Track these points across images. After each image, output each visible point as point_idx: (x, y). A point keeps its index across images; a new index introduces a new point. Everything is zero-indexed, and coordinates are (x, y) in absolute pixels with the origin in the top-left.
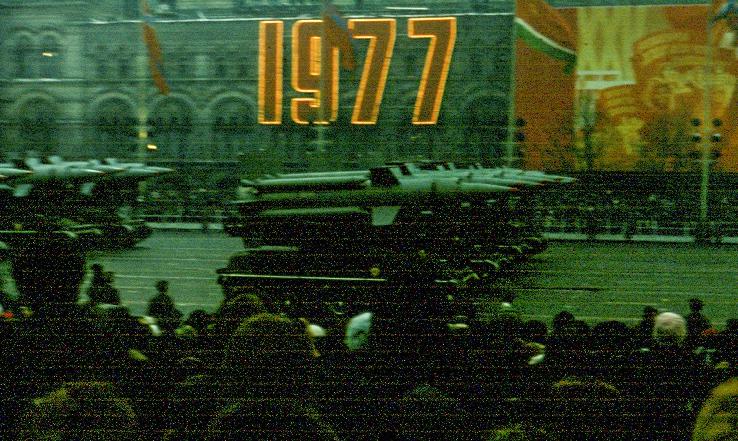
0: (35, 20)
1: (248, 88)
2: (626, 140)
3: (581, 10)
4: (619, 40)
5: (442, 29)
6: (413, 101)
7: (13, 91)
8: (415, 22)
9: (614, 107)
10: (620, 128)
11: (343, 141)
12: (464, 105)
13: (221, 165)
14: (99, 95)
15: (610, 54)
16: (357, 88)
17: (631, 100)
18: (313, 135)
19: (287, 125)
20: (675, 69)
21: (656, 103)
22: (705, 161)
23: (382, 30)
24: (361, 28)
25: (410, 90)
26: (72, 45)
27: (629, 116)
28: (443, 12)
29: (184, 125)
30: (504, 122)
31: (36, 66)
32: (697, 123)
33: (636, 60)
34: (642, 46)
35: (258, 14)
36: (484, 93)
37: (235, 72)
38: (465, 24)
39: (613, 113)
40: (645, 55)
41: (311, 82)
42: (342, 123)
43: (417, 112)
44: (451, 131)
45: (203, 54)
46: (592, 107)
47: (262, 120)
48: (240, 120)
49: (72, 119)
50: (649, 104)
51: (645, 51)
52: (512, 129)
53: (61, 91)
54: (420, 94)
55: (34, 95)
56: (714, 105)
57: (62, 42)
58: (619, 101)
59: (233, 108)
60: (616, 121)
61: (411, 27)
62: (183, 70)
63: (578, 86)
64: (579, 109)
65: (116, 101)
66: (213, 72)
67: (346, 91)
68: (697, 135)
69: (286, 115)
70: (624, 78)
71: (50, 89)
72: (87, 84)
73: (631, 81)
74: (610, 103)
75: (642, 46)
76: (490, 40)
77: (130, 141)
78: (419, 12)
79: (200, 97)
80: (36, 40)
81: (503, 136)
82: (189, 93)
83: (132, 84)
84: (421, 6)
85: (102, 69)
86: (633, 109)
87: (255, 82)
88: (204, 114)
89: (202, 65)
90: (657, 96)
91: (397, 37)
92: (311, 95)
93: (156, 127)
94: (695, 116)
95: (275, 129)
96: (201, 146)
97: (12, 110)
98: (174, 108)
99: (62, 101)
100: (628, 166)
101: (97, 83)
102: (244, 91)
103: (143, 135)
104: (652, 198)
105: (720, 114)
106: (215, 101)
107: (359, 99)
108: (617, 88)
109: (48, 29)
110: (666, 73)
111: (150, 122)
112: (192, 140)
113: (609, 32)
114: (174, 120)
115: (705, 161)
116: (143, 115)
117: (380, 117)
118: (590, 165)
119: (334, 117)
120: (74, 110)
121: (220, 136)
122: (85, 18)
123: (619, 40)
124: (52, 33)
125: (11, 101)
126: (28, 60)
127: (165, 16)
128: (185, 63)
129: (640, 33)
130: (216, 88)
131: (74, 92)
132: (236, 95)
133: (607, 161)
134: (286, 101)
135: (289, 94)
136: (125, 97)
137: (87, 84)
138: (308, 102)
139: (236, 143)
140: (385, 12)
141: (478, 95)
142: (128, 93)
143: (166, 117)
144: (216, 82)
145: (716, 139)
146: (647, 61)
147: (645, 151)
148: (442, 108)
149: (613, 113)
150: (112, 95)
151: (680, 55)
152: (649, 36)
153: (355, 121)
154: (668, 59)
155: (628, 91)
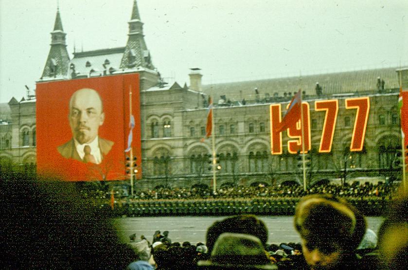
0: (160, 111)
1: (265, 137)
5: (363, 104)
6: (350, 139)
7: (149, 145)
8: (348, 101)
11: (315, 161)
12: (377, 140)
13: (253, 175)
14: (192, 144)
16: (321, 135)
18: (300, 159)
19: (286, 155)
23: (332, 106)
24: (320, 105)
25: (348, 134)
26: (177, 121)
28: (362, 95)
29: (235, 157)
30: (400, 148)
31: (161, 133)
35: (267, 101)
36: (386, 133)
37: (258, 129)
38: (375, 101)
41: (298, 133)
42: (313, 152)
44: (370, 154)
45: (241, 122)
47: (272, 152)
48: (262, 153)
49: (177, 156)
53: (172, 143)
55: (160, 146)
57: (172, 120)
59: (258, 147)
61: (346, 103)
62: (232, 130)
65: (200, 147)
66: (248, 130)
67: (315, 136)
69: (285, 148)
71: (168, 142)
72: (185, 139)
76: (388, 107)
77: (207, 165)
78: (350, 96)
79: (242, 143)
80: (160, 120)
81: (400, 154)
82: (236, 142)
85: (192, 131)
87: (268, 134)
88: (244, 151)
89: (242, 128)
92: (298, 139)
93: (220, 158)
95: (280, 156)
96: (243, 166)
97: (149, 154)
98: (229, 148)
99: (173, 148)
101: (190, 139)
102: (263, 139)
103: (214, 162)
106: (249, 144)
107: (322, 140)
111: (218, 156)
112: (239, 164)
114: (229, 154)
116: (214, 154)
117: (332, 148)
119: (310, 149)
120: (179, 152)
121: (252, 161)
122: (184, 108)
125: (147, 149)
126: (156, 128)
127: (222, 105)
128: (233, 127)
130: (250, 138)
131: (180, 143)
132: (260, 141)
134: (285, 143)
135: (286, 139)
136: (203, 145)
137: (185, 139)
138: (296, 143)
139: (260, 163)
140: (332, 97)
141: (382, 135)
142: (206, 143)
143: (225, 153)
144: (248, 135)
148: (365, 140)
150: (198, 144)
153: (320, 151)
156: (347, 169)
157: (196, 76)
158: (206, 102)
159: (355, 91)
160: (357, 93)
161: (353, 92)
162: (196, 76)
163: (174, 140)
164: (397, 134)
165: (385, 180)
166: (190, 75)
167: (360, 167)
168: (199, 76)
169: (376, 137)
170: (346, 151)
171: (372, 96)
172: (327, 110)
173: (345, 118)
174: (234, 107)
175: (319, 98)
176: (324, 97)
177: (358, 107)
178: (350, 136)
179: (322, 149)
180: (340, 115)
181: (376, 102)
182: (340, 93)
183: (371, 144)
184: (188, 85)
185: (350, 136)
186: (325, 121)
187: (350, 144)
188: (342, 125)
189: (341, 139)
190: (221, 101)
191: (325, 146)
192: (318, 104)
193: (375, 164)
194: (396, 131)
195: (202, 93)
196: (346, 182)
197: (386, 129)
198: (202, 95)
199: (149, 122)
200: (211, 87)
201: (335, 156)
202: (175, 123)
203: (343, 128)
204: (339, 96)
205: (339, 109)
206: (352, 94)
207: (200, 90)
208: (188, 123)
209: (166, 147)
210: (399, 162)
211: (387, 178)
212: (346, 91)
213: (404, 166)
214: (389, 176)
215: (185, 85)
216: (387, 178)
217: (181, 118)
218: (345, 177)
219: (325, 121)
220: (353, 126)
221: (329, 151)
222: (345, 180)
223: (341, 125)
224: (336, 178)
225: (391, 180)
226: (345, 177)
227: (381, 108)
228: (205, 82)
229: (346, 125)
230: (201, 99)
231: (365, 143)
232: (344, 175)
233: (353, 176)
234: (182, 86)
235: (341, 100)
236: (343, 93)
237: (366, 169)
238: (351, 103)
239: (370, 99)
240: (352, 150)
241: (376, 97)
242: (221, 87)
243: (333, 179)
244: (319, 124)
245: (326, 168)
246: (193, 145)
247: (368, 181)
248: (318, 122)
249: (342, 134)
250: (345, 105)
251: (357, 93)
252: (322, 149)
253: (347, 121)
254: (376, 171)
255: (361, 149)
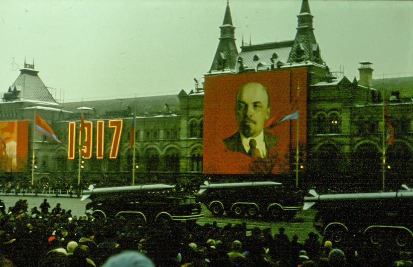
0: (327, 106)
14: (360, 141)
53: (339, 139)
55: (327, 142)
57: (340, 116)
80: (328, 116)
83: (377, 136)
103: (384, 161)
109: (333, 110)
120: (347, 149)
124: (336, 112)
150: (367, 141)
157: (366, 71)
158: (375, 97)
162: (366, 71)
163: (342, 136)
166: (359, 70)
168: (370, 71)
174: (406, 103)
184: (358, 79)
190: (393, 98)
195: (372, 89)
198: (373, 91)
199: (316, 117)
200: (383, 83)
202: (343, 119)
207: (371, 85)
208: (356, 120)
209: (333, 143)
215: (355, 79)
217: (349, 114)
228: (376, 76)
230: (370, 96)
234: (352, 81)
242: (393, 81)
246: (361, 143)
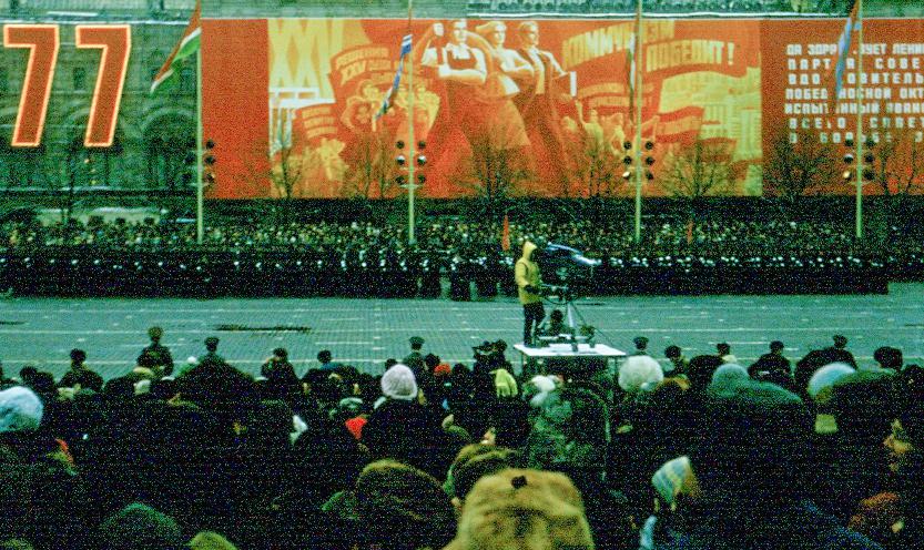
2: (327, 163)
3: (272, 22)
4: (315, 57)
5: (115, 39)
6: (84, 120)
9: (315, 127)
10: (318, 150)
12: (143, 127)
15: (305, 64)
17: (331, 120)
20: (377, 86)
21: (354, 119)
22: (411, 187)
23: (43, 39)
25: (81, 107)
27: (329, 137)
28: (115, 19)
30: (192, 144)
32: (401, 145)
33: (334, 78)
34: (340, 61)
36: (165, 111)
38: (143, 34)
39: (311, 134)
40: (344, 72)
43: (88, 133)
44: (129, 155)
46: (289, 128)
50: (350, 125)
51: (342, 67)
52: (200, 152)
54: (93, 111)
56: (418, 126)
58: (317, 121)
60: (315, 143)
61: (78, 36)
63: (271, 105)
64: (273, 130)
68: (401, 158)
70: (322, 96)
73: (332, 101)
74: (307, 124)
75: (340, 61)
78: (87, 19)
81: (191, 160)
84: (89, 11)
86: (332, 130)
90: (359, 117)
91: (61, 46)
94: (397, 140)
100: (331, 194)
104: (354, 225)
105: (424, 137)
107: (19, 117)
108: (314, 107)
110: (365, 90)
113: (304, 44)
115: (411, 187)
118: (288, 191)
123: (315, 57)
129: (338, 47)
133: (308, 189)
140: (46, 18)
141: (157, 113)
145: (420, 163)
146: (346, 78)
147: (347, 176)
148: (118, 124)
149: (311, 134)
151: (382, 72)
152: (345, 52)
153: (15, 143)
154: (367, 75)
155: (327, 110)
156: (76, 189)
159: (101, 7)
160: (104, 14)
161: (93, 10)
164: (188, 114)
165: (159, 215)
167: (107, 184)
169: (143, 117)
170: (75, 146)
171: (137, 22)
172: (33, 47)
173: (76, 70)
175: (15, 18)
176: (28, 14)
177: (105, 48)
178: (83, 112)
179: (19, 140)
180: (64, 62)
181: (146, 38)
182: (67, 10)
183: (133, 133)
185: (83, 112)
186: (28, 73)
187: (85, 130)
188: (68, 86)
189: (65, 116)
191: (27, 132)
192: (12, 31)
193: (140, 178)
194: (185, 106)
196: (73, 216)
197: (165, 101)
201: (50, 155)
203: (69, 93)
204: (64, 18)
205: (62, 51)
206: (94, 14)
210: (188, 177)
211: (164, 211)
212: (81, 7)
213: (200, 185)
214: (167, 207)
216: (164, 211)
218: (70, 204)
219: (28, 73)
220: (93, 88)
221: (36, 144)
222: (70, 211)
223: (66, 84)
224: (53, 206)
225: (175, 213)
226: (70, 205)
227: (155, 53)
229: (77, 87)
231: (118, 130)
232: (66, 201)
233: (89, 205)
235: (67, 26)
236: (71, 10)
237: (119, 189)
238: (88, 35)
239: (132, 29)
240: (88, 144)
241: (145, 25)
243: (44, 211)
244: (12, 78)
245: (30, 183)
247: (122, 216)
248: (11, 74)
249: (64, 108)
250: (74, 41)
251: (104, 14)
252: (19, 140)
253: (79, 77)
254: (141, 193)
255: (109, 143)
